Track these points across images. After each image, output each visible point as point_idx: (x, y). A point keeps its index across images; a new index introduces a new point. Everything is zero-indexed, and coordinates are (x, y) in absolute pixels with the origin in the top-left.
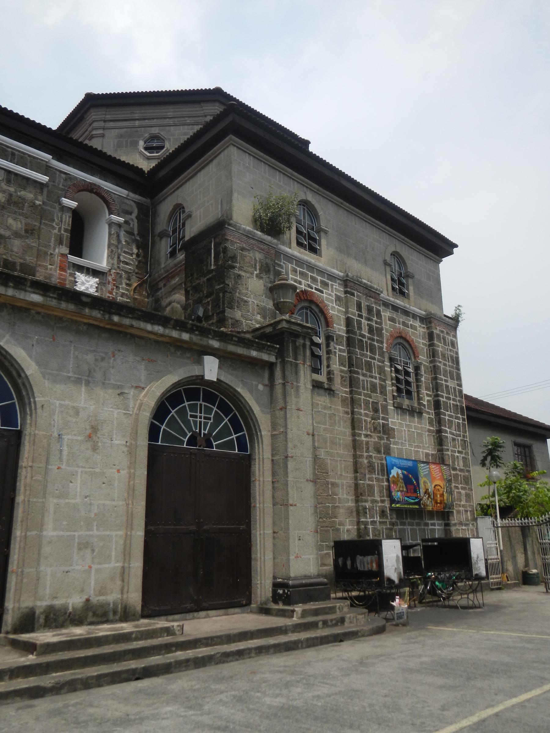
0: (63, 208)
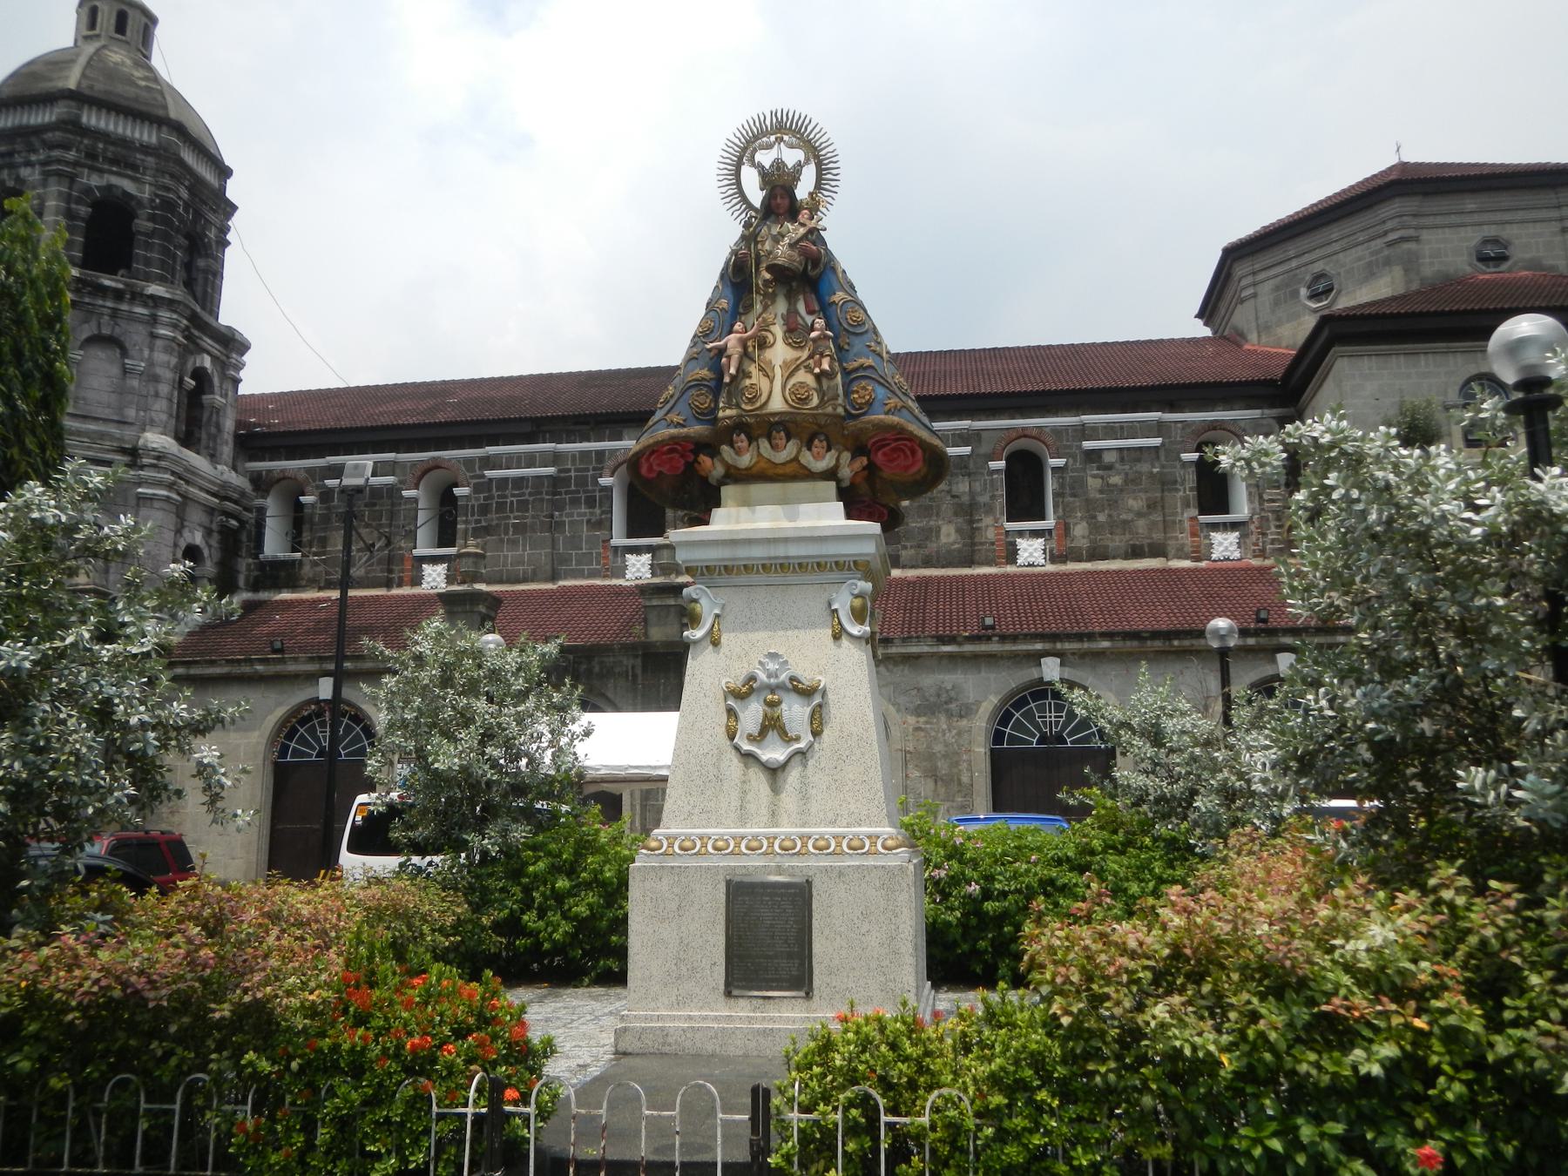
0: (1185, 464)
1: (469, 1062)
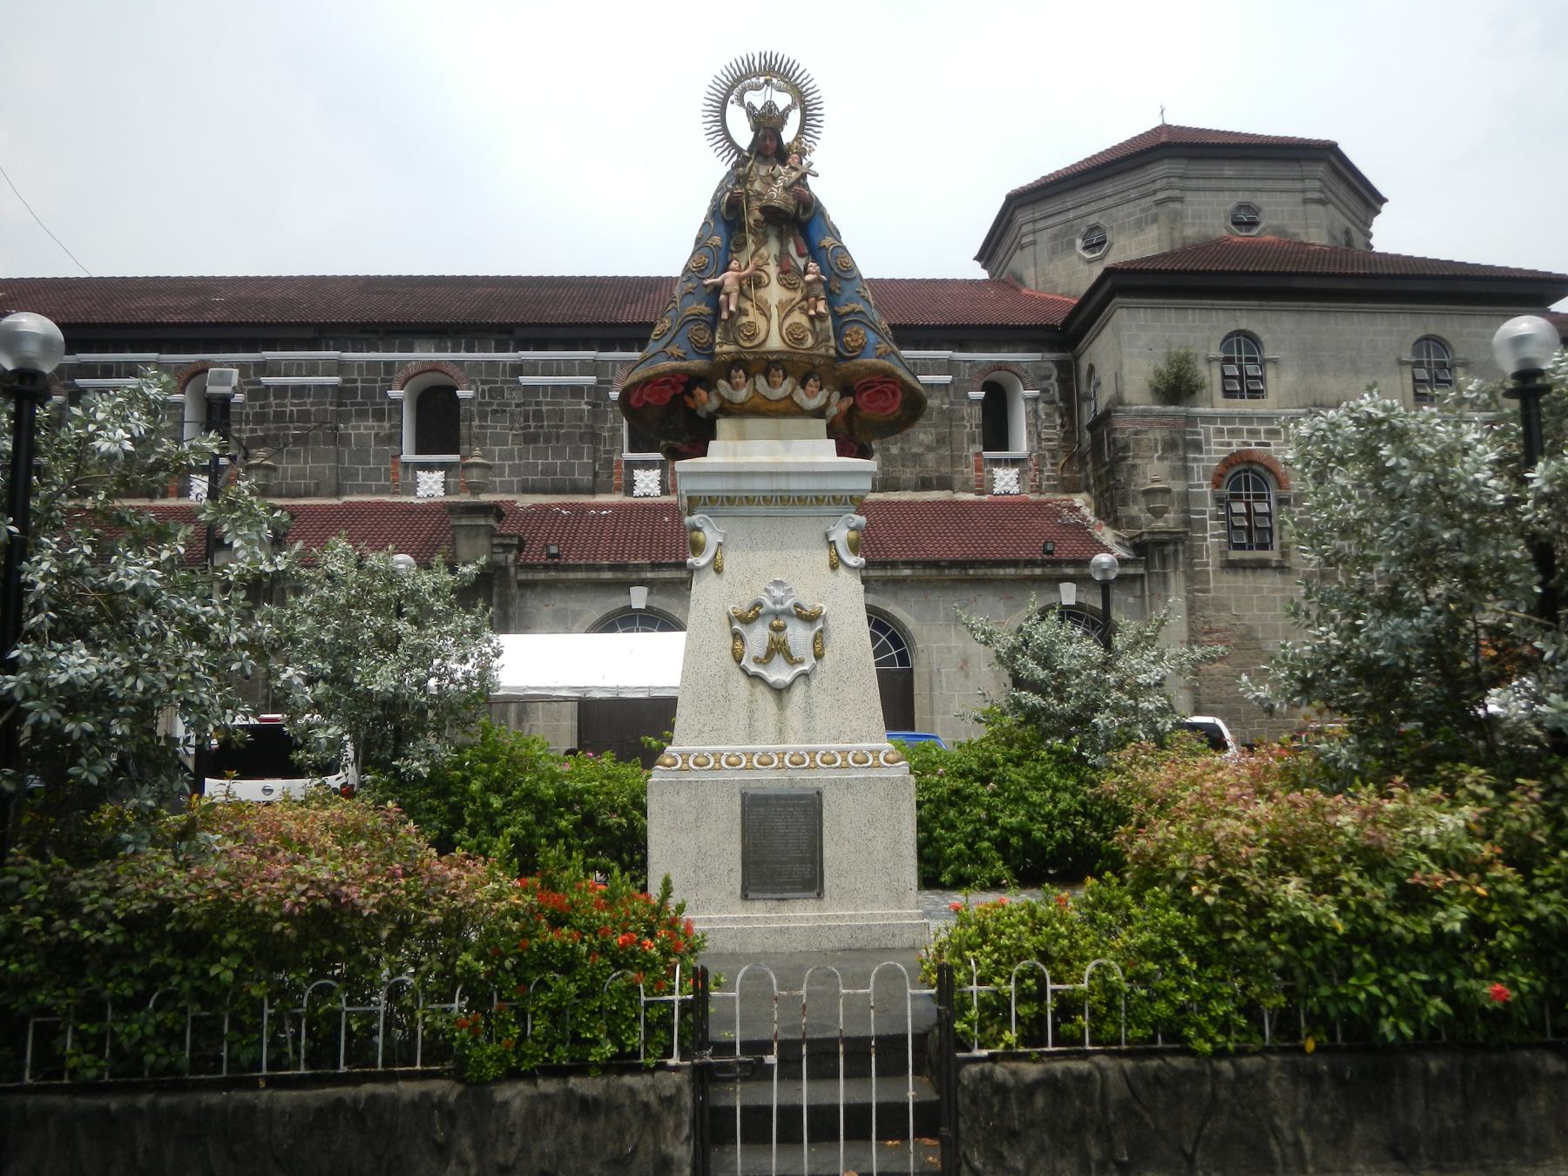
0: (972, 402)
1: (666, 954)
